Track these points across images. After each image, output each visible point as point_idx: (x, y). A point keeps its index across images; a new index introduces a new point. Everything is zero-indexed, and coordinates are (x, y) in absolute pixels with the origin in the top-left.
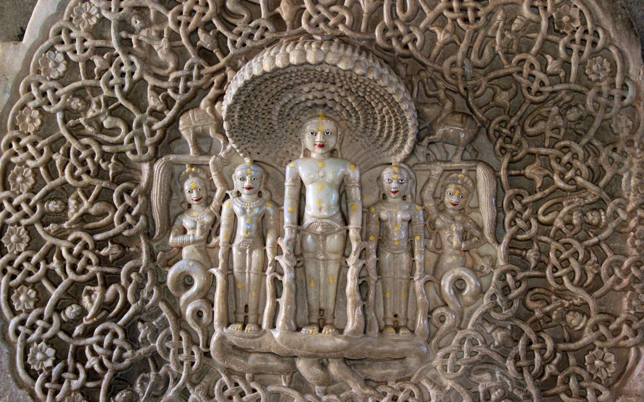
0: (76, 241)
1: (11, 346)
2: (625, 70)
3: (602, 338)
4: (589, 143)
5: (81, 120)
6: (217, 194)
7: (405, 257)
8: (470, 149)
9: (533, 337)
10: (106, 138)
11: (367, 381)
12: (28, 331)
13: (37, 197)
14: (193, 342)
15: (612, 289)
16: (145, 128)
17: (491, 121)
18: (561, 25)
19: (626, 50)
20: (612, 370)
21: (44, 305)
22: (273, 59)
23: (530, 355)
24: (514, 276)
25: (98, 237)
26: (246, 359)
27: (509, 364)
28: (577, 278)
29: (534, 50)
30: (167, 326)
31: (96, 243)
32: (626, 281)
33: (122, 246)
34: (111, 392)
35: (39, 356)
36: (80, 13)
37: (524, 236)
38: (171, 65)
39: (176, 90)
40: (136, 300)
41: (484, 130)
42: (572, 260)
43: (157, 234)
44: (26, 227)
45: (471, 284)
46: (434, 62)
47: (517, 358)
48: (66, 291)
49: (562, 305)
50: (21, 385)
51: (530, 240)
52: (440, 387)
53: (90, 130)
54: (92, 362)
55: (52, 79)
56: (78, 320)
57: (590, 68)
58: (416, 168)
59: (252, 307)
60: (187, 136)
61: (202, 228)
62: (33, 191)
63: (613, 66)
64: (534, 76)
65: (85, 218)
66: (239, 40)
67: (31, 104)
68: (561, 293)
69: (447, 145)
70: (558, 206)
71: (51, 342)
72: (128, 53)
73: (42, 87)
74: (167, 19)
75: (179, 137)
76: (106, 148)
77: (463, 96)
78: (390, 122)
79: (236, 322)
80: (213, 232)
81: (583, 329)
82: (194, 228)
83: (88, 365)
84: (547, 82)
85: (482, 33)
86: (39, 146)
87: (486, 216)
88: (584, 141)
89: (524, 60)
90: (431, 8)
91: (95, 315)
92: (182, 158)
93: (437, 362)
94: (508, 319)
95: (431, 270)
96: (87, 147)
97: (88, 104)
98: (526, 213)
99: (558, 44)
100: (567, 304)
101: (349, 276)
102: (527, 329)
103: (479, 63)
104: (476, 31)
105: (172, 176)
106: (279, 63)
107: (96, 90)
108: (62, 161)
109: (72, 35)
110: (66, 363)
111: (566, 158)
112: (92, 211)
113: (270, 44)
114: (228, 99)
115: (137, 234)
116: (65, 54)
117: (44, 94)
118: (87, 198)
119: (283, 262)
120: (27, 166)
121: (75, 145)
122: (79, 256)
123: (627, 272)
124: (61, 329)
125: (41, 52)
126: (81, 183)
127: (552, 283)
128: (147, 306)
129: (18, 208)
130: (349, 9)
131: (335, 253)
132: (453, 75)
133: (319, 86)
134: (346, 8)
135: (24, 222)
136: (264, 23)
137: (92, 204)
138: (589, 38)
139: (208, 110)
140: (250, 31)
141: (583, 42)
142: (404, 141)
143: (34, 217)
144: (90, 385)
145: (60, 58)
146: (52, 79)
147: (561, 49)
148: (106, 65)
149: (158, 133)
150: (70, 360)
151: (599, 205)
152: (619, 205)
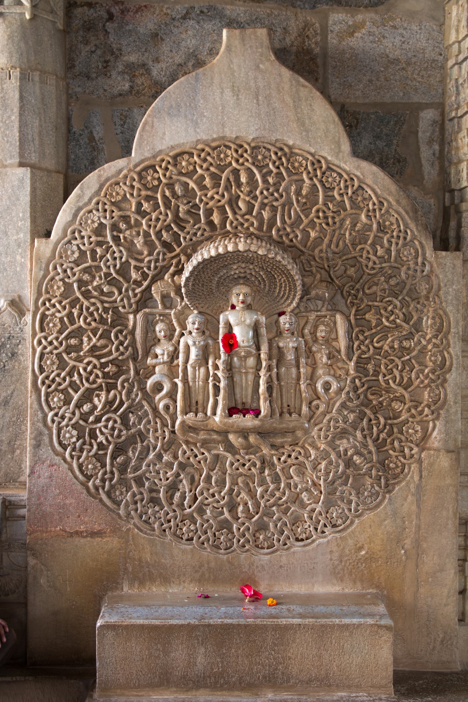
0: (89, 363)
1: (50, 429)
2: (424, 254)
3: (413, 416)
4: (403, 299)
5: (90, 287)
6: (177, 333)
7: (294, 370)
8: (331, 303)
9: (372, 417)
10: (106, 299)
11: (273, 446)
12: (60, 420)
13: (63, 336)
14: (164, 425)
15: (418, 386)
16: (130, 292)
17: (344, 286)
18: (385, 227)
19: (424, 242)
20: (419, 435)
21: (70, 404)
22: (217, 248)
23: (370, 428)
24: (360, 380)
25: (103, 360)
26: (198, 434)
27: (359, 434)
28: (397, 381)
29: (369, 242)
30: (148, 415)
31: (101, 364)
32: (426, 382)
33: (117, 366)
34: (114, 458)
35: (67, 435)
36: (87, 220)
37: (366, 356)
38: (146, 253)
39: (149, 268)
40: (128, 400)
41: (339, 291)
42: (394, 370)
43: (140, 358)
44: (57, 355)
45: (335, 386)
46: (308, 250)
47: (363, 430)
48: (83, 395)
49: (389, 397)
50: (57, 453)
51: (369, 358)
52: (317, 449)
53: (95, 294)
54: (101, 438)
55: (70, 262)
56: (91, 412)
57: (403, 253)
58: (299, 315)
59: (200, 402)
60: (157, 297)
61: (168, 354)
62: (60, 332)
63: (417, 252)
64: (369, 258)
65: (93, 349)
66: (188, 237)
67: (57, 278)
68: (388, 390)
69: (317, 301)
70: (385, 338)
71: (74, 427)
72: (118, 245)
73: (64, 267)
74: (142, 224)
75: (151, 297)
76: (106, 305)
77: (326, 271)
78: (285, 287)
79: (190, 412)
80: (175, 357)
81: (401, 411)
82: (163, 354)
83: (99, 440)
84: (377, 262)
85: (337, 232)
86: (63, 304)
87: (342, 343)
88: (400, 298)
89: (363, 249)
90: (307, 217)
91: (102, 409)
92: (154, 311)
93: (314, 433)
94: (357, 406)
95: (309, 378)
96: (94, 304)
97: (94, 277)
98: (367, 342)
99: (382, 238)
100: (392, 396)
101: (261, 382)
102: (368, 412)
103: (336, 250)
104: (334, 231)
105: (148, 322)
106: (221, 250)
107: (98, 268)
108: (78, 313)
109: (82, 234)
110: (85, 439)
111: (390, 308)
112: (98, 344)
113: (207, 239)
114: (186, 274)
115: (127, 358)
116: (78, 245)
117: (65, 271)
118: (95, 336)
119: (220, 374)
120: (56, 317)
121: (86, 303)
122: (91, 373)
123: (427, 377)
124: (81, 418)
125: (63, 245)
126: (91, 327)
127: (383, 384)
128: (135, 403)
129: (51, 343)
130: (255, 217)
131: (252, 368)
132: (321, 258)
133: (243, 265)
134: (254, 217)
135: (55, 352)
136: (204, 226)
137: (98, 340)
138: (402, 235)
139: (170, 280)
140: (195, 231)
141: (398, 237)
142: (293, 299)
143: (61, 349)
144: (100, 452)
145: (75, 248)
146: (70, 262)
147: (385, 241)
148: (105, 252)
149: (139, 295)
150: (87, 437)
151: (410, 337)
152: (421, 336)
